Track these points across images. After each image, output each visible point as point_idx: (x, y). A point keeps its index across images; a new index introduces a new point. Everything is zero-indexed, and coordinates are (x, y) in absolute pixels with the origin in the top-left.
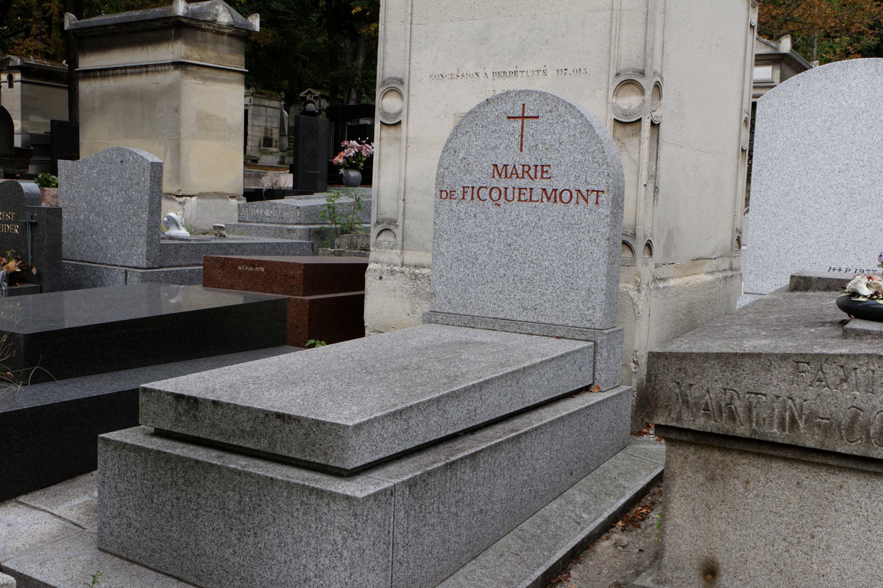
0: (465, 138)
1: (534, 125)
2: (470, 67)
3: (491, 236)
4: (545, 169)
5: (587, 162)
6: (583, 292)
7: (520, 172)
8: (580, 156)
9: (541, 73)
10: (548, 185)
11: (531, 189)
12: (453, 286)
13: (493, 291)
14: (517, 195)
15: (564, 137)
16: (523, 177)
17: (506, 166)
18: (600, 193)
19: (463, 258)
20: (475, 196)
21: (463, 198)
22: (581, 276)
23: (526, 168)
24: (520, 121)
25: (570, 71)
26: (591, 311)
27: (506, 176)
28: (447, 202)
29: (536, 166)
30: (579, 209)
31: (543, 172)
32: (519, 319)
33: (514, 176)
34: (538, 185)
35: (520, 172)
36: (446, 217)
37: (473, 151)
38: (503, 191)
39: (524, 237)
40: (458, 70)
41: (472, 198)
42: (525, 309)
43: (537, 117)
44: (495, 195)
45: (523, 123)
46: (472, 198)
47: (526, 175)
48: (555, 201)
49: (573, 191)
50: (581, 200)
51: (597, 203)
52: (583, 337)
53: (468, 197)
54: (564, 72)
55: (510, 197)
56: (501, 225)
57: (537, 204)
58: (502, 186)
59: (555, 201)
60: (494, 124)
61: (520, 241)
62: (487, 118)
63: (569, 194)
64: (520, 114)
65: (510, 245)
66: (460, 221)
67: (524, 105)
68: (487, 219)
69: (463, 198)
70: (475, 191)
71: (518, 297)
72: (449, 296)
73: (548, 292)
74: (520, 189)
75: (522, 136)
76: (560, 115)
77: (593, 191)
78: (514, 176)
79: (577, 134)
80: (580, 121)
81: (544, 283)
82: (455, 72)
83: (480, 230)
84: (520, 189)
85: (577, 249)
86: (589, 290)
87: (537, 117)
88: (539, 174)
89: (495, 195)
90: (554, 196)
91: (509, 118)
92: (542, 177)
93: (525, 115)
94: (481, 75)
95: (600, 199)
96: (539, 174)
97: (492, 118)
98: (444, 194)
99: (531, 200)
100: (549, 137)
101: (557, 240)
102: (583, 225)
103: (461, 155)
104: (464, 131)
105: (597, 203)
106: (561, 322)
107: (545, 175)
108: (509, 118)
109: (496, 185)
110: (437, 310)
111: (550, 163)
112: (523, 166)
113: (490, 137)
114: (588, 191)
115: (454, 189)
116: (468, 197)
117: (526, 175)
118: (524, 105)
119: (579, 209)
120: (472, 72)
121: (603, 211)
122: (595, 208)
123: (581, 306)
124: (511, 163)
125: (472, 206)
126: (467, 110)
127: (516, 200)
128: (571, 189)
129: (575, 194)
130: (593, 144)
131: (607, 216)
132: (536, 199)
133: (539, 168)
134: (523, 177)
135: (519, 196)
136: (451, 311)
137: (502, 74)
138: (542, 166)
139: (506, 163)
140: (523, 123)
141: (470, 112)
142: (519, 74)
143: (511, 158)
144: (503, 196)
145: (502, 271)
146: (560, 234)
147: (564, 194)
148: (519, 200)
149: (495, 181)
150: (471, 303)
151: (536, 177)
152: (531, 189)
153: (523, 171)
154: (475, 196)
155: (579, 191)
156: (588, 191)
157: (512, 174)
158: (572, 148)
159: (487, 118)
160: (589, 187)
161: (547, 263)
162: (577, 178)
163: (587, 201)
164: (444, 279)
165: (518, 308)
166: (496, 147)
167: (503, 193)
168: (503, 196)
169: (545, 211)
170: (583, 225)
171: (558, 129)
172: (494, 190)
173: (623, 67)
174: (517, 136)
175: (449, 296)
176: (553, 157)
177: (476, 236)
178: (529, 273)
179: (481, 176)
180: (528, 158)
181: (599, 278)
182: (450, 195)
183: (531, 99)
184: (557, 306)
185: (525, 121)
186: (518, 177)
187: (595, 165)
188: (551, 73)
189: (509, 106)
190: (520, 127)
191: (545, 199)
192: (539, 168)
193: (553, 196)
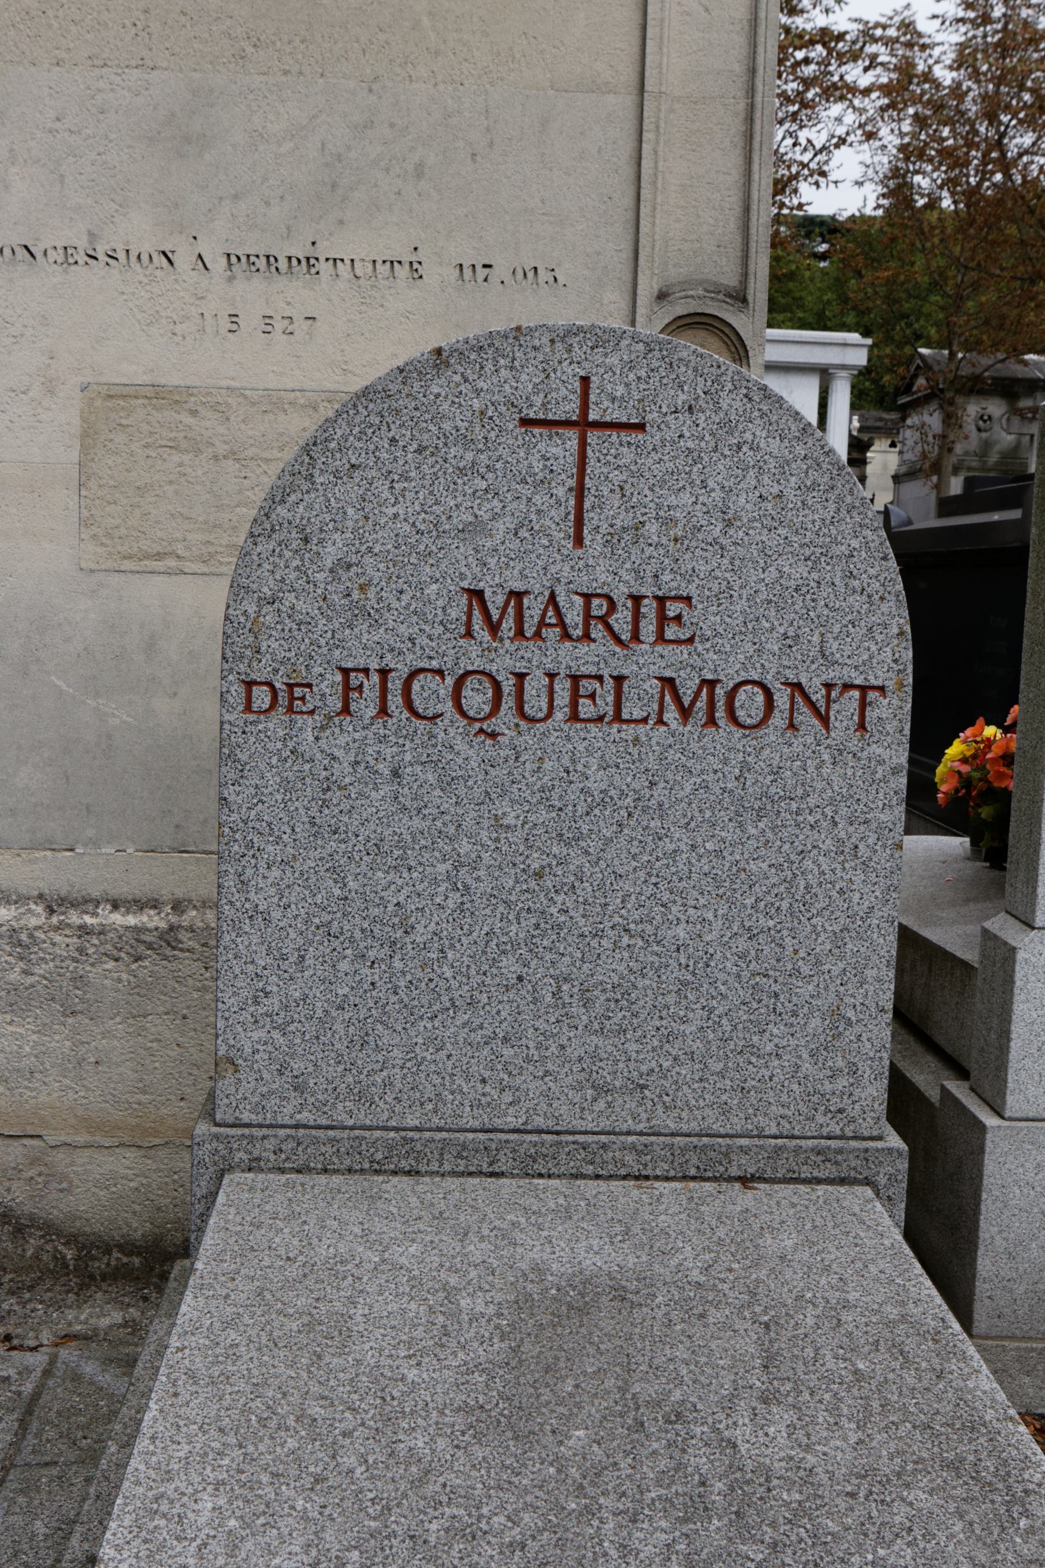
0: (350, 490)
1: (628, 455)
2: (137, 229)
3: (465, 847)
4: (673, 609)
5: (826, 591)
6: (815, 1023)
7: (574, 617)
8: (803, 569)
9: (402, 272)
10: (683, 666)
11: (619, 680)
12: (311, 1029)
13: (477, 1037)
14: (563, 698)
15: (743, 503)
16: (587, 636)
17: (517, 596)
18: (872, 695)
19: (352, 926)
20: (395, 701)
21: (346, 710)
22: (806, 970)
23: (598, 607)
24: (572, 436)
25: (502, 270)
26: (842, 1082)
27: (520, 633)
28: (275, 724)
29: (637, 600)
30: (797, 748)
31: (662, 619)
32: (579, 1124)
33: (552, 634)
34: (647, 664)
35: (574, 617)
36: (272, 780)
37: (383, 541)
38: (508, 686)
39: (594, 846)
40: (92, 236)
41: (383, 711)
42: (602, 1090)
43: (641, 427)
44: (476, 699)
45: (583, 444)
46: (383, 711)
47: (598, 631)
48: (711, 721)
49: (776, 686)
50: (804, 716)
51: (862, 726)
52: (828, 1171)
53: (366, 706)
54: (482, 273)
55: (536, 703)
56: (503, 807)
57: (641, 729)
58: (502, 665)
59: (711, 721)
60: (467, 442)
61: (577, 860)
62: (438, 418)
63: (760, 698)
64: (570, 409)
65: (539, 875)
66: (335, 796)
67: (585, 381)
68: (447, 784)
69: (346, 710)
70: (395, 685)
71: (575, 1051)
72: (297, 1065)
73: (689, 1029)
74: (575, 679)
75: (580, 492)
76: (727, 425)
77: (847, 687)
78: (552, 634)
79: (790, 493)
80: (800, 450)
81: (671, 999)
82: (83, 243)
83: (417, 823)
84: (575, 679)
85: (791, 883)
86: (836, 1013)
87: (641, 427)
88: (648, 628)
89: (476, 699)
90: (709, 704)
91: (526, 422)
92: (661, 638)
93: (593, 416)
94: (184, 260)
95: (871, 714)
96: (648, 628)
97: (457, 420)
98: (261, 697)
99: (618, 717)
100: (686, 498)
101: (719, 853)
102: (812, 801)
103: (331, 554)
104: (340, 463)
105: (862, 726)
106: (738, 1124)
107: (671, 632)
108: (526, 422)
109: (478, 664)
110: (246, 1117)
111: (692, 590)
112: (587, 597)
113: (452, 488)
114: (829, 686)
115: (303, 676)
116: (366, 706)
117: (598, 631)
118: (585, 381)
119: (797, 748)
120: (146, 248)
121: (886, 754)
122: (854, 744)
123: (807, 1067)
124: (537, 585)
125: (383, 739)
126: (357, 384)
127: (559, 716)
128: (769, 679)
129: (782, 699)
130: (847, 528)
131: (895, 771)
132: (637, 714)
133: (649, 608)
134: (587, 636)
135: (574, 704)
136: (304, 1117)
137: (261, 263)
138: (661, 600)
139: (518, 586)
140: (583, 444)
141: (366, 393)
142: (324, 267)
143: (544, 567)
144: (508, 703)
145: (510, 966)
146: (730, 833)
147: (741, 696)
148: (574, 716)
149: (474, 651)
150: (388, 1084)
151: (636, 637)
152: (619, 680)
153: (588, 616)
154: (395, 701)
155: (798, 687)
156: (829, 686)
157: (542, 623)
158: (772, 541)
159: (438, 418)
160: (832, 675)
161: (681, 932)
162: (790, 641)
163: (825, 720)
164: (273, 1003)
165: (579, 1087)
166: (474, 528)
167: (508, 693)
168: (508, 703)
169: (672, 755)
170: (812, 801)
171: (719, 472)
172: (471, 682)
173: (674, 274)
174: (561, 492)
175: (297, 1065)
176: (703, 568)
177: (401, 844)
178: (614, 967)
179: (414, 627)
180: (603, 571)
181: (870, 973)
182: (290, 697)
183: (613, 360)
184: (721, 1075)
185: (592, 437)
186: (566, 636)
187: (857, 601)
188: (437, 273)
189: (528, 379)
190: (572, 460)
191: (671, 715)
192: (649, 608)
193: (701, 704)
